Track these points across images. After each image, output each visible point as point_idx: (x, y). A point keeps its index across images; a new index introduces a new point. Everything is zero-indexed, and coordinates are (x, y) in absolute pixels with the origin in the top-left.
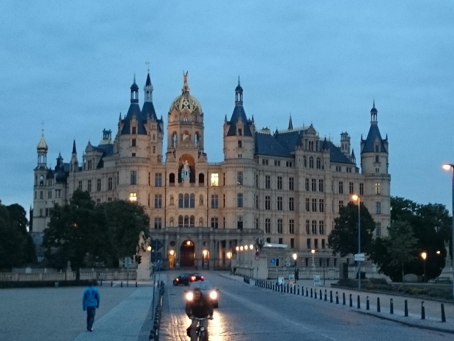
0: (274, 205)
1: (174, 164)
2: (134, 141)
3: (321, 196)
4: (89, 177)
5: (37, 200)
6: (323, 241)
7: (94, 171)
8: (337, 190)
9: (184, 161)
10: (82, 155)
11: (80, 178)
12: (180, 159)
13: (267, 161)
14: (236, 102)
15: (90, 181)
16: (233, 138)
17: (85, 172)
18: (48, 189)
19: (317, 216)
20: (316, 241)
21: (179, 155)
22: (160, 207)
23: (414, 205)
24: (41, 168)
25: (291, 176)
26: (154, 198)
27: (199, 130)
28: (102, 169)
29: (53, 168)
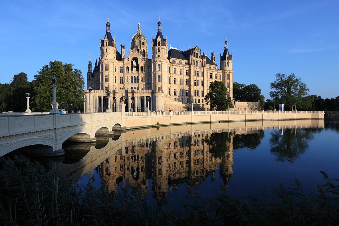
0: (178, 82)
2: (107, 49)
3: (202, 79)
6: (202, 100)
8: (209, 76)
9: (134, 61)
13: (175, 61)
16: (156, 47)
19: (200, 88)
20: (199, 99)
22: (122, 83)
23: (242, 85)
24: (89, 72)
25: (188, 69)
26: (119, 79)
27: (145, 50)
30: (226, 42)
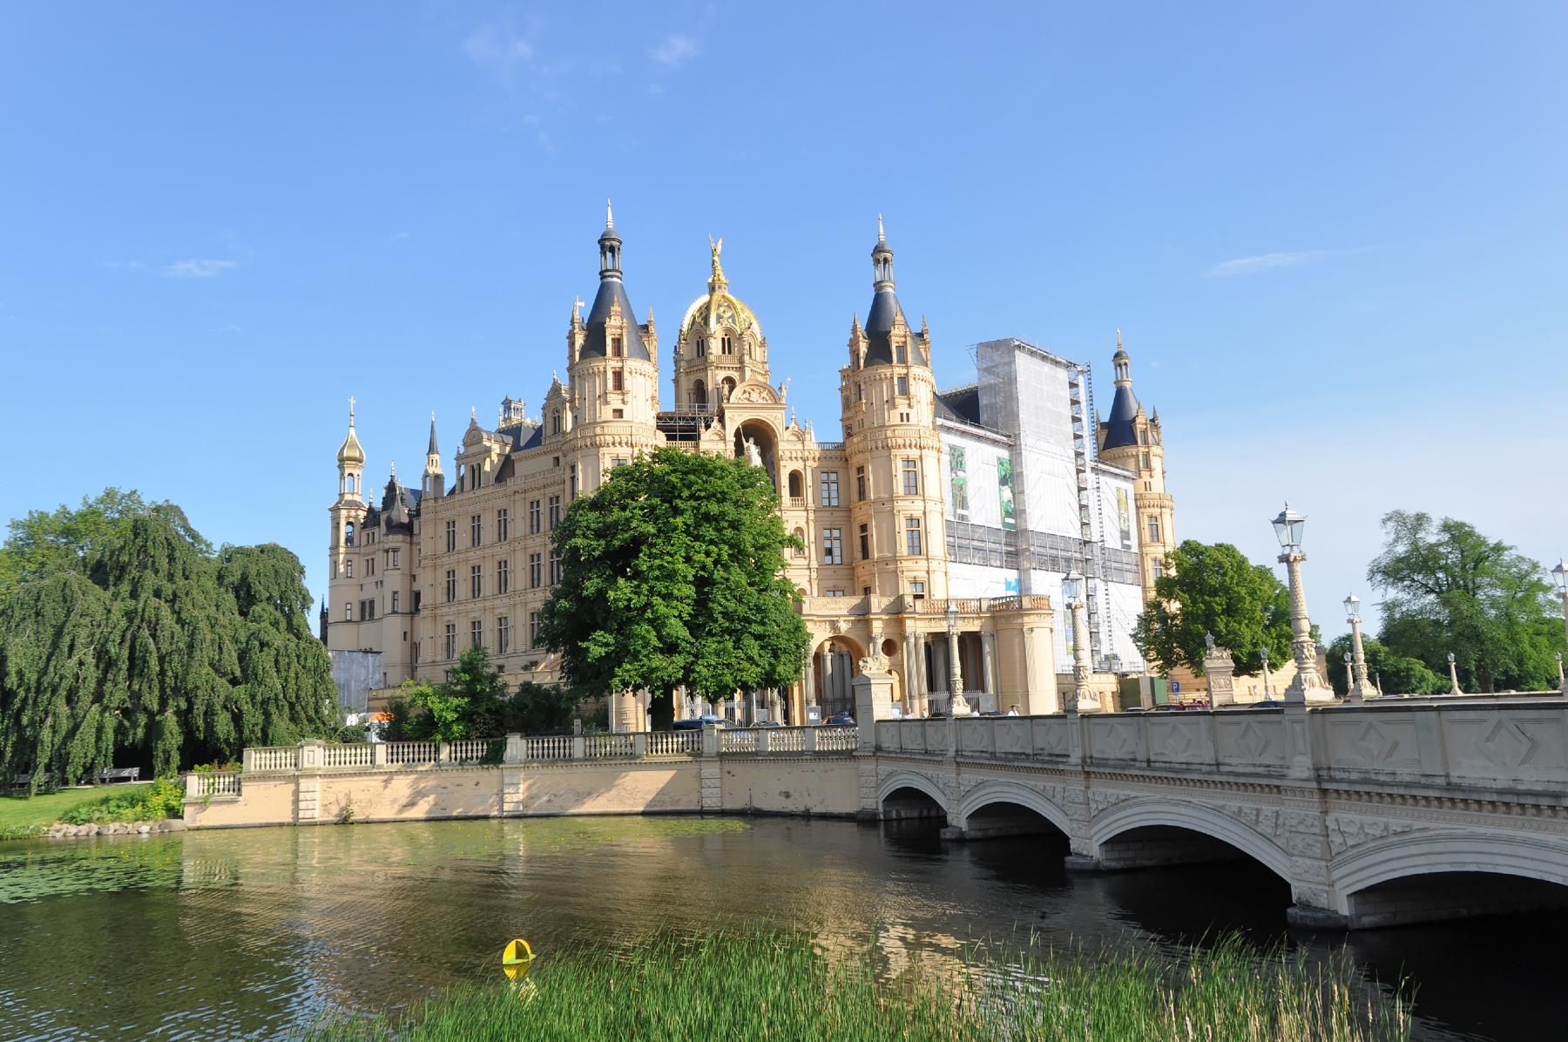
1: (721, 446)
2: (618, 376)
4: (474, 509)
5: (336, 582)
7: (490, 490)
9: (747, 441)
10: (455, 455)
11: (447, 515)
12: (737, 434)
14: (874, 285)
15: (476, 518)
16: (884, 371)
17: (466, 496)
18: (365, 555)
21: (734, 420)
28: (510, 482)
29: (378, 505)
30: (1118, 355)
